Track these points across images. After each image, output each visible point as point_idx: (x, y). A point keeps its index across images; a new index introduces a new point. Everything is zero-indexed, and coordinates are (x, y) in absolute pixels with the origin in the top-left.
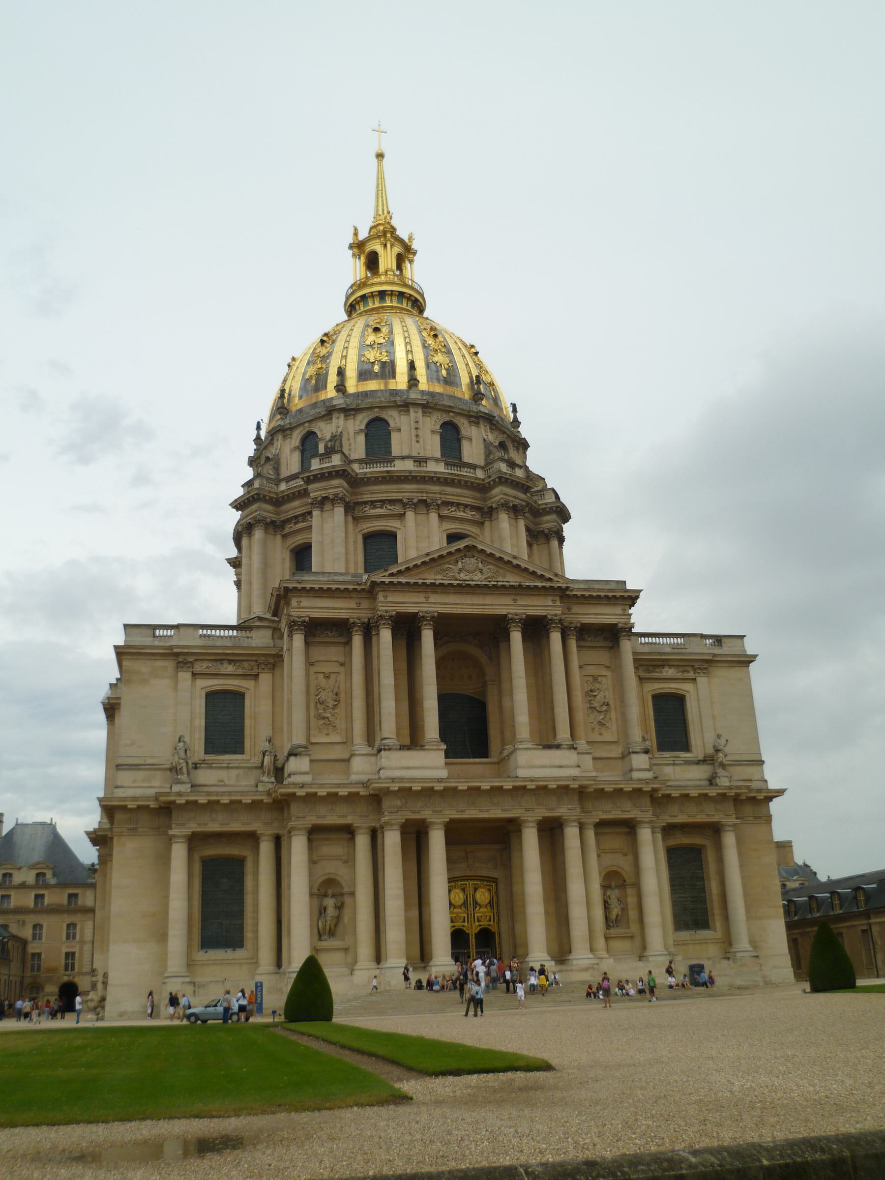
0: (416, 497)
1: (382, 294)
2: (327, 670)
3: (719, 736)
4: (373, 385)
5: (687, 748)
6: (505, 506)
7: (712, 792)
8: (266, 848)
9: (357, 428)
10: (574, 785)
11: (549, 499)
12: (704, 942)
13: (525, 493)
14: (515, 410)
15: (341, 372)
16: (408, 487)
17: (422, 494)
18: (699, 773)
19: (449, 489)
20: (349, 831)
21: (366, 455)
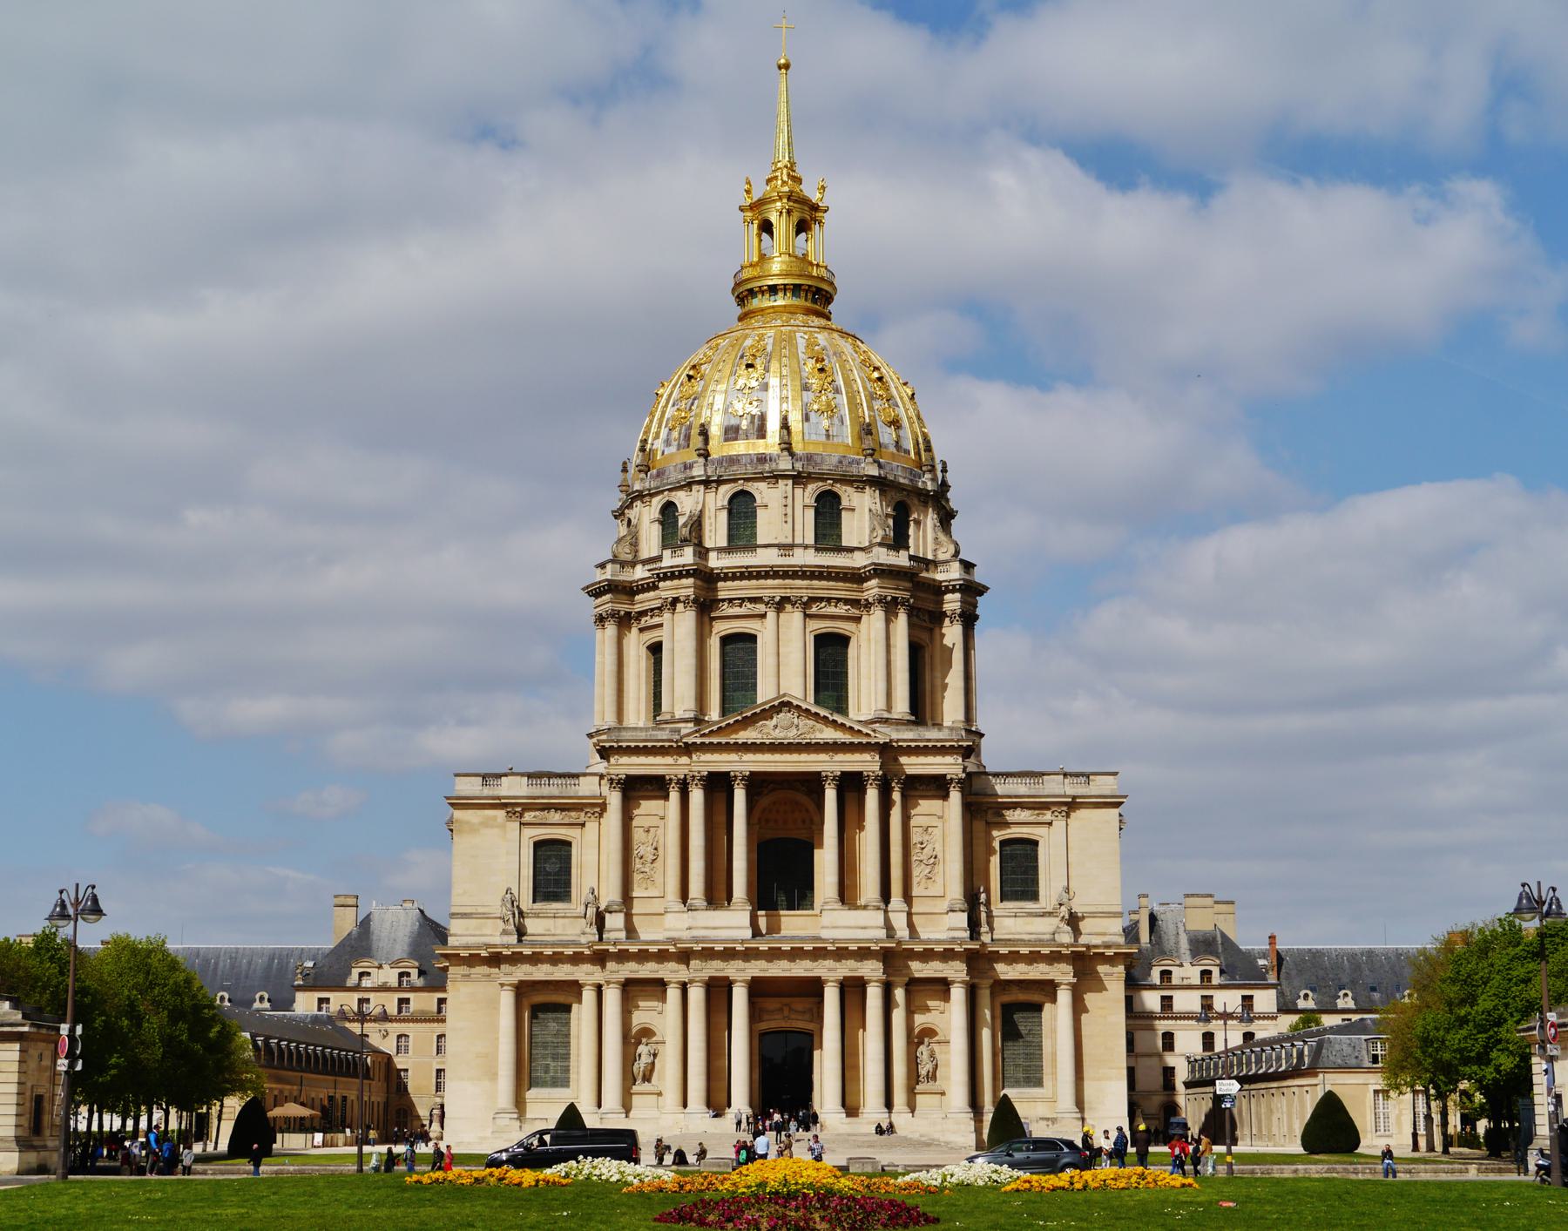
0: (778, 594)
1: (773, 290)
2: (646, 825)
3: (1067, 890)
4: (739, 448)
5: (1033, 896)
6: (881, 600)
7: (1045, 951)
8: (588, 995)
9: (719, 504)
10: (874, 947)
11: (953, 573)
12: (1034, 1100)
13: (911, 581)
14: (928, 449)
15: (704, 433)
16: (770, 582)
17: (790, 587)
18: (1041, 928)
19: (815, 583)
20: (660, 985)
21: (730, 537)
